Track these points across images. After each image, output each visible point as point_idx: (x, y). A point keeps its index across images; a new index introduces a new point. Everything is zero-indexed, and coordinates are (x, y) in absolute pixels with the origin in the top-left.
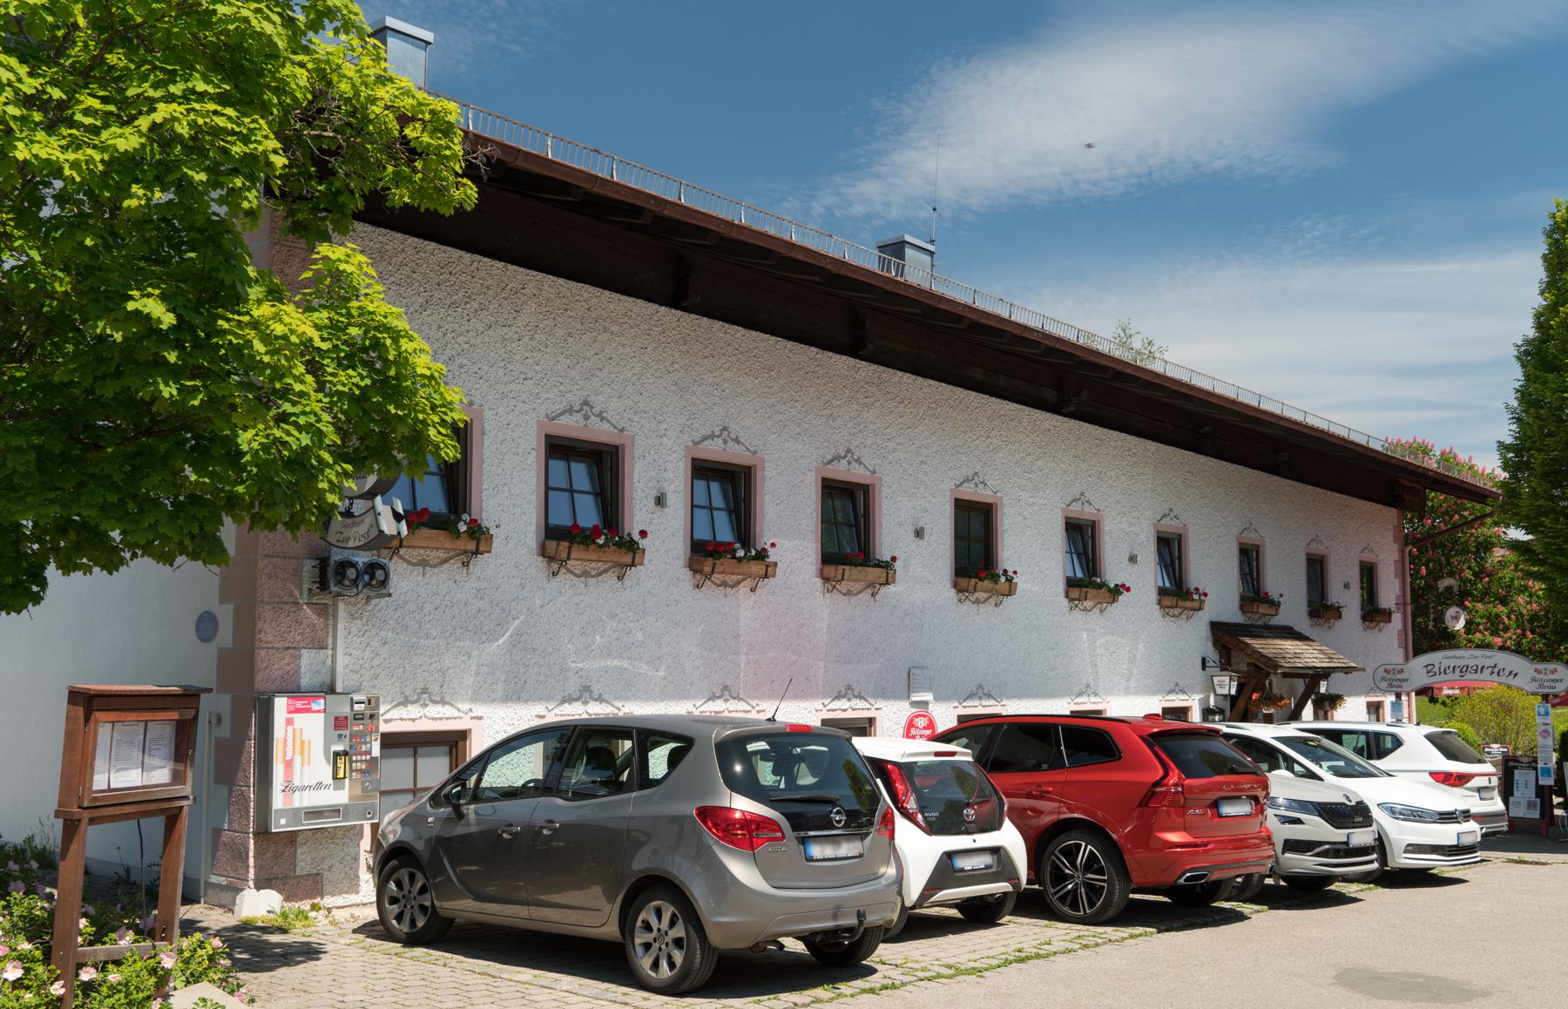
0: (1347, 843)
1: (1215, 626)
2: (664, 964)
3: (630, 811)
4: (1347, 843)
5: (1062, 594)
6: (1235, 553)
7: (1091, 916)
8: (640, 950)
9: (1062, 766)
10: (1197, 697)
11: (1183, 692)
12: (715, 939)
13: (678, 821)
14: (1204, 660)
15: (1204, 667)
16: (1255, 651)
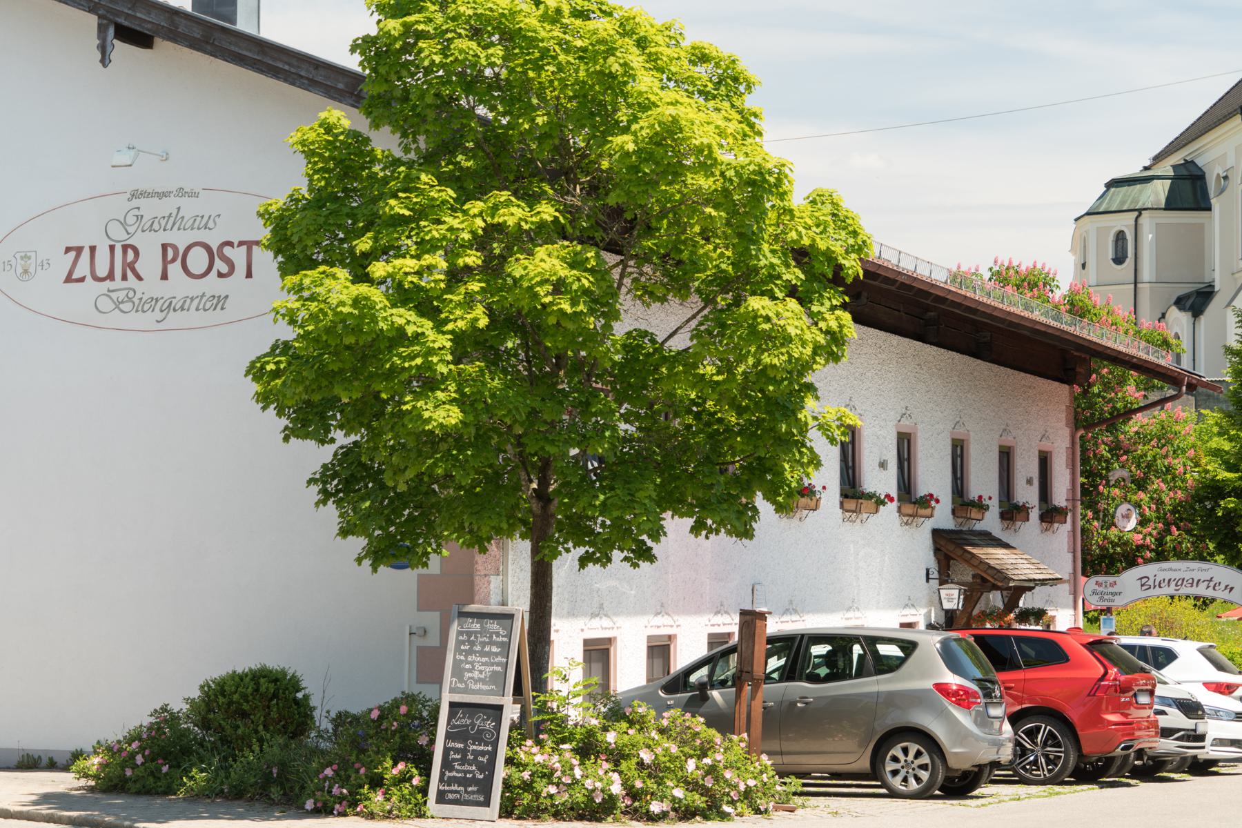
0: (1195, 730)
1: (936, 533)
2: (912, 781)
3: (874, 689)
4: (1195, 730)
5: (838, 506)
6: (949, 442)
7: (1050, 778)
8: (889, 776)
9: (1020, 667)
10: (923, 611)
11: (796, 611)
12: (953, 763)
13: (925, 691)
14: (928, 570)
15: (928, 579)
16: (981, 562)
